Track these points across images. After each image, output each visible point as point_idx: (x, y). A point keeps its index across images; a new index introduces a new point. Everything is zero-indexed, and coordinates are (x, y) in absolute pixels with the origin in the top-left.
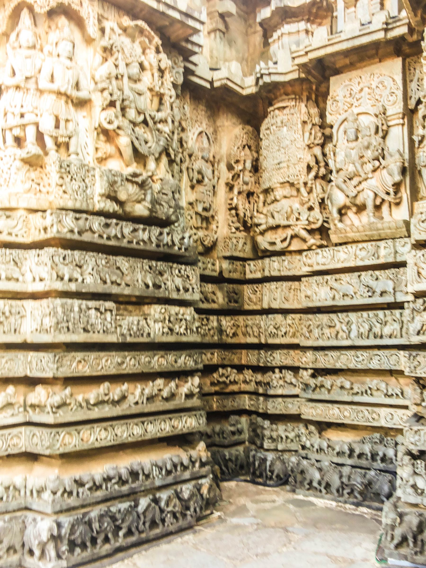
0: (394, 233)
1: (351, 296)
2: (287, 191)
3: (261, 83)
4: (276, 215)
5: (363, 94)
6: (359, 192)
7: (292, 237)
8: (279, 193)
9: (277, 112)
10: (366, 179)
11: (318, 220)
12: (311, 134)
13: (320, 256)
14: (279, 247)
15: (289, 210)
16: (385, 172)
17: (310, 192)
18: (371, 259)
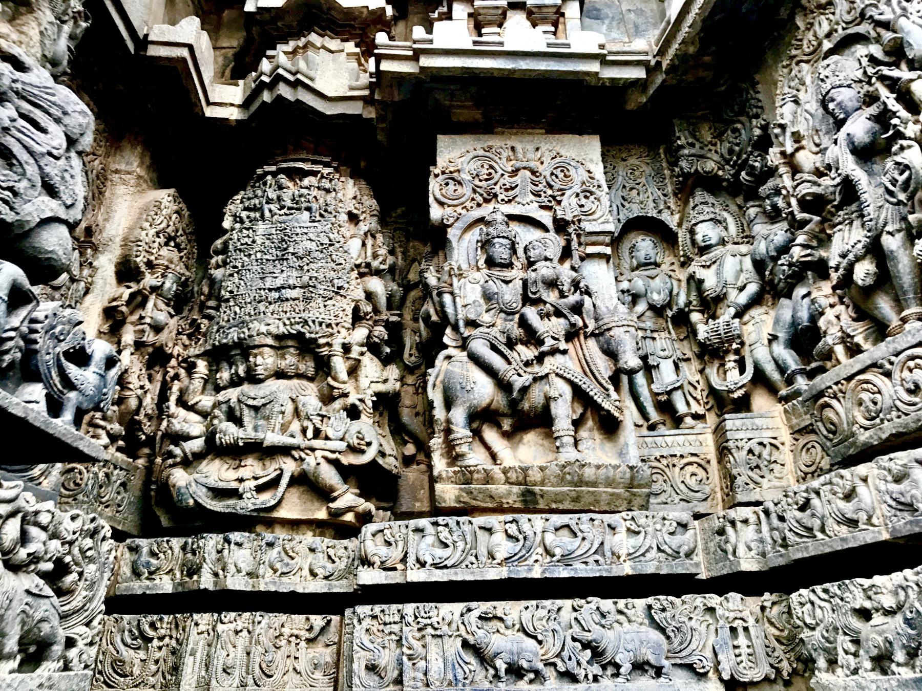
0: (618, 496)
1: (532, 676)
2: (290, 360)
3: (266, 97)
4: (248, 417)
5: (517, 180)
6: (535, 380)
7: (294, 481)
8: (265, 361)
9: (283, 179)
10: (554, 351)
11: (369, 444)
12: (364, 245)
13: (430, 539)
14: (250, 503)
15: (289, 408)
16: (592, 344)
17: (353, 371)
18: (591, 560)
